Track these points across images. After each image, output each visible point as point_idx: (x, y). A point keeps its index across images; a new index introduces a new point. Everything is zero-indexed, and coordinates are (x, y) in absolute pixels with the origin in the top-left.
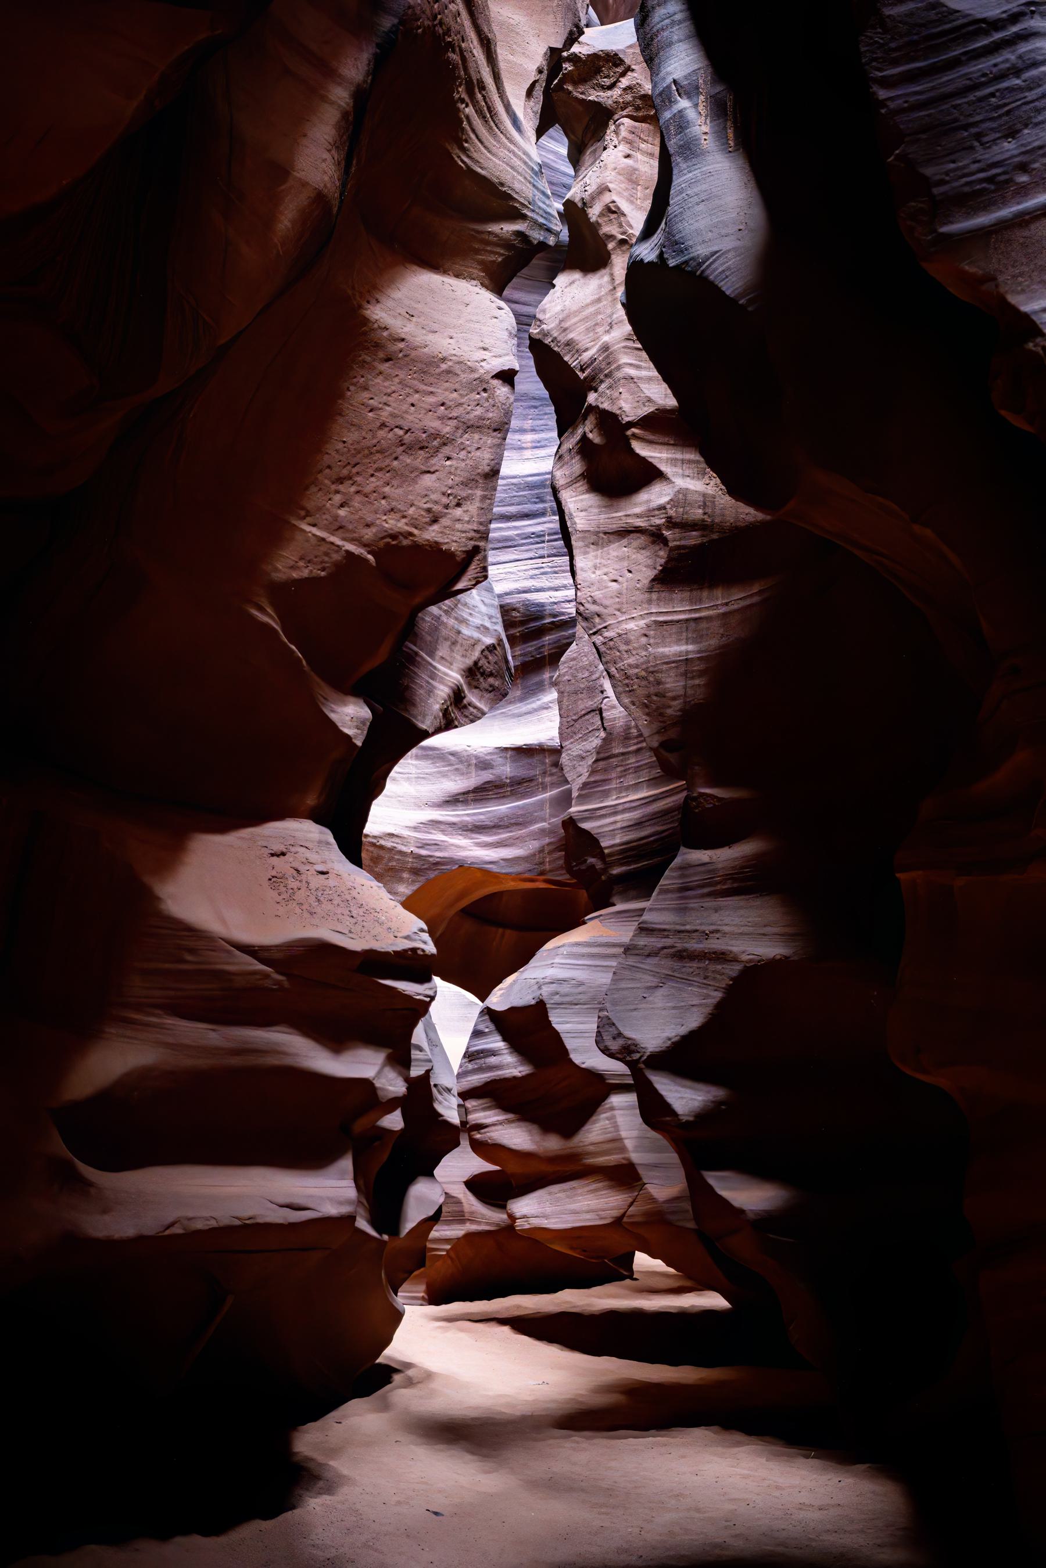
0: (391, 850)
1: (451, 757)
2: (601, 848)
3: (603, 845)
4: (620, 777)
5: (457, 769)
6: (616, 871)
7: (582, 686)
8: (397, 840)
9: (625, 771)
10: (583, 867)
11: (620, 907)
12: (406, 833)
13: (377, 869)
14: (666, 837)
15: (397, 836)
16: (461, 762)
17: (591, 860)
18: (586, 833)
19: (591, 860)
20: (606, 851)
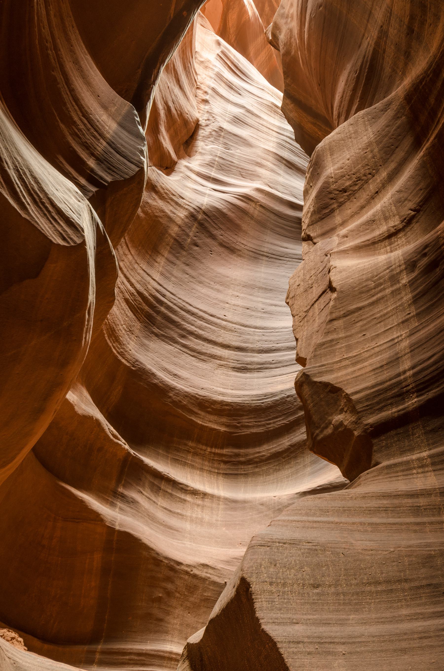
0: (204, 580)
1: (261, 507)
2: (347, 396)
3: (349, 391)
4: (361, 332)
5: (266, 515)
6: (371, 420)
7: (310, 282)
8: (210, 571)
9: (365, 325)
10: (329, 431)
11: (385, 463)
12: (220, 566)
13: (192, 599)
14: (435, 363)
15: (213, 568)
16: (269, 509)
17: (338, 418)
18: (326, 385)
19: (338, 418)
20: (354, 397)
